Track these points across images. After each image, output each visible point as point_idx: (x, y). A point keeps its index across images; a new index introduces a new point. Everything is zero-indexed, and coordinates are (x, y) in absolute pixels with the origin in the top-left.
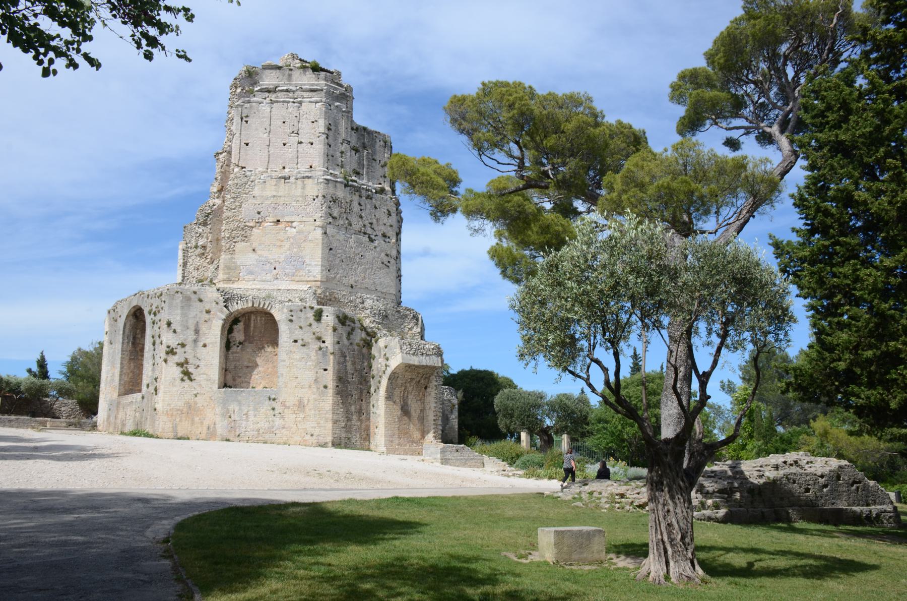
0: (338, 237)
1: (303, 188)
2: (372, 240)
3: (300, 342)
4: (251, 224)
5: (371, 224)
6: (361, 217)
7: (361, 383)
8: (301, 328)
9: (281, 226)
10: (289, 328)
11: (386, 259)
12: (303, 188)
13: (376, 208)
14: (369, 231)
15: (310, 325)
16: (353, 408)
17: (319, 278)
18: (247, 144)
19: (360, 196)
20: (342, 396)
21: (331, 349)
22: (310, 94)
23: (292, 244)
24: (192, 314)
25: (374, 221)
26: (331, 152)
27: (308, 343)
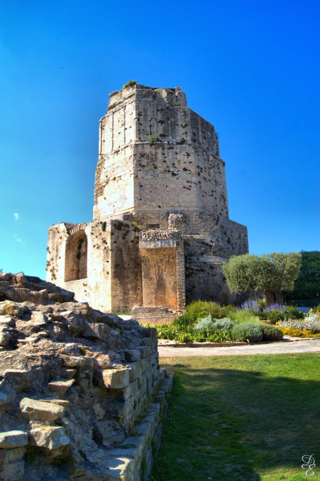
0: (147, 177)
1: (125, 154)
2: (174, 174)
3: (96, 246)
4: (104, 184)
5: (174, 164)
6: (165, 161)
7: (136, 268)
8: (97, 237)
9: (117, 179)
10: (92, 239)
11: (187, 185)
12: (125, 154)
13: (177, 153)
14: (172, 169)
15: (101, 234)
16: (129, 286)
17: (133, 206)
18: (104, 141)
19: (163, 149)
20: (119, 279)
21: (110, 248)
22: (129, 99)
23: (121, 189)
24: (55, 241)
25: (176, 162)
26: (142, 128)
27: (100, 246)
